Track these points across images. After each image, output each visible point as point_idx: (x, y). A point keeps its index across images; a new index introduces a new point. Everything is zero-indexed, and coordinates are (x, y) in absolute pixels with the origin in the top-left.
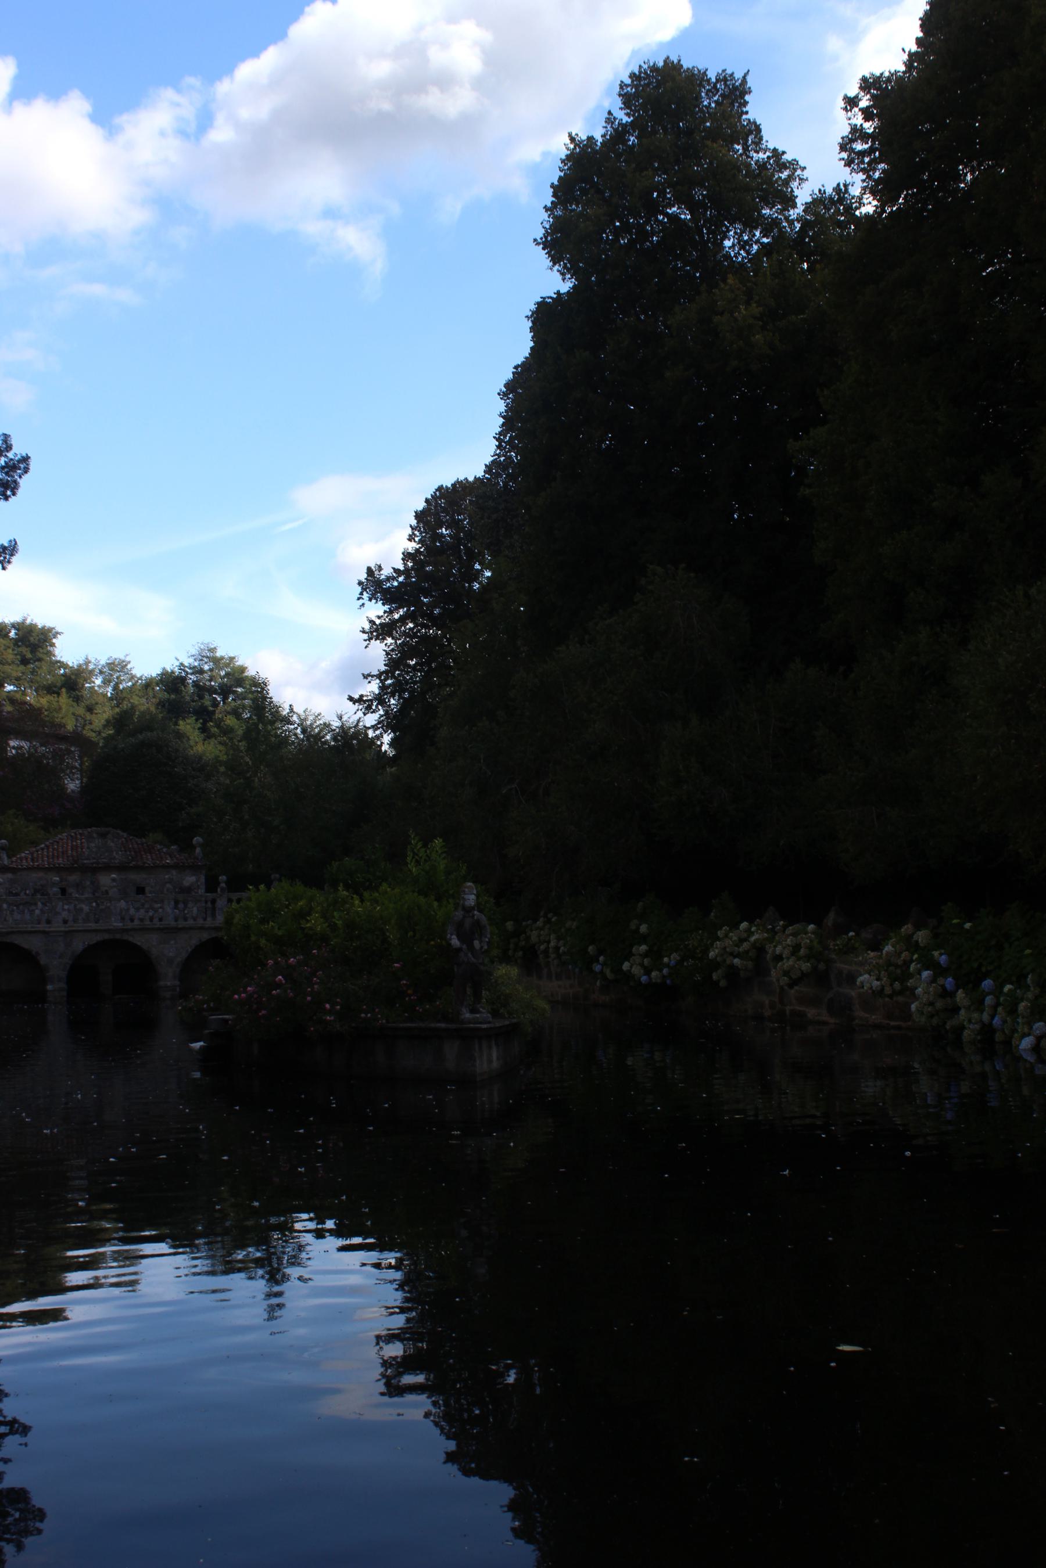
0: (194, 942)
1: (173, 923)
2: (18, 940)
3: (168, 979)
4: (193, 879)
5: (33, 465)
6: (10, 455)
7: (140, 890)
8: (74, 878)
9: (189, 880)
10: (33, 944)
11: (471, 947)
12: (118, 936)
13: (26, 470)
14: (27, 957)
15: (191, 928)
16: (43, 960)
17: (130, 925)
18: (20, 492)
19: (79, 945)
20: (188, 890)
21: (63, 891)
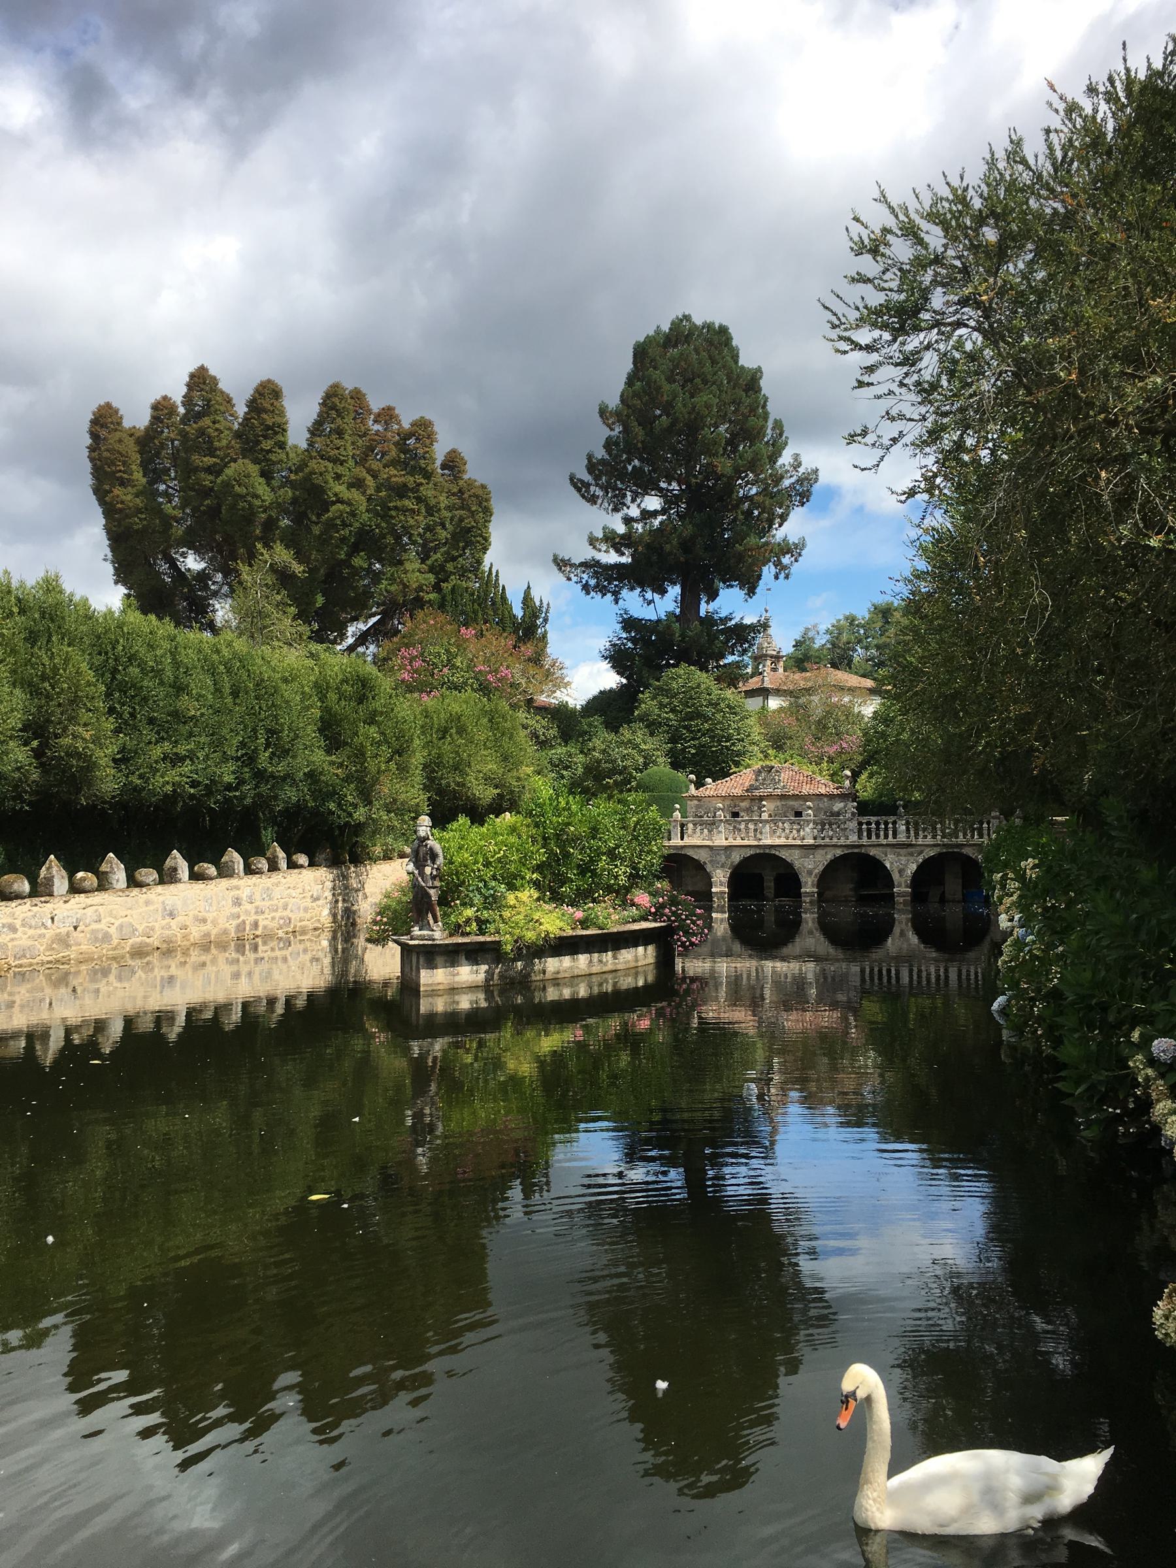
0: (830, 857)
1: (812, 842)
2: (690, 853)
3: (809, 887)
4: (842, 805)
5: (820, 474)
6: (801, 470)
7: (798, 814)
8: (744, 804)
9: (838, 806)
10: (702, 856)
11: (422, 874)
12: (767, 851)
13: (816, 480)
14: (699, 867)
15: (826, 846)
16: (709, 868)
17: (778, 842)
18: (812, 498)
19: (736, 858)
20: (838, 814)
21: (735, 815)
